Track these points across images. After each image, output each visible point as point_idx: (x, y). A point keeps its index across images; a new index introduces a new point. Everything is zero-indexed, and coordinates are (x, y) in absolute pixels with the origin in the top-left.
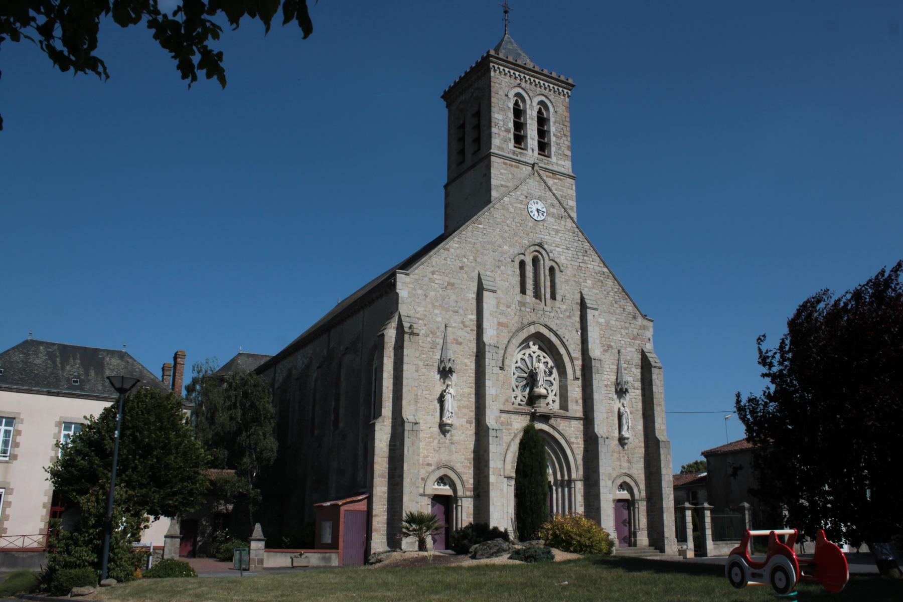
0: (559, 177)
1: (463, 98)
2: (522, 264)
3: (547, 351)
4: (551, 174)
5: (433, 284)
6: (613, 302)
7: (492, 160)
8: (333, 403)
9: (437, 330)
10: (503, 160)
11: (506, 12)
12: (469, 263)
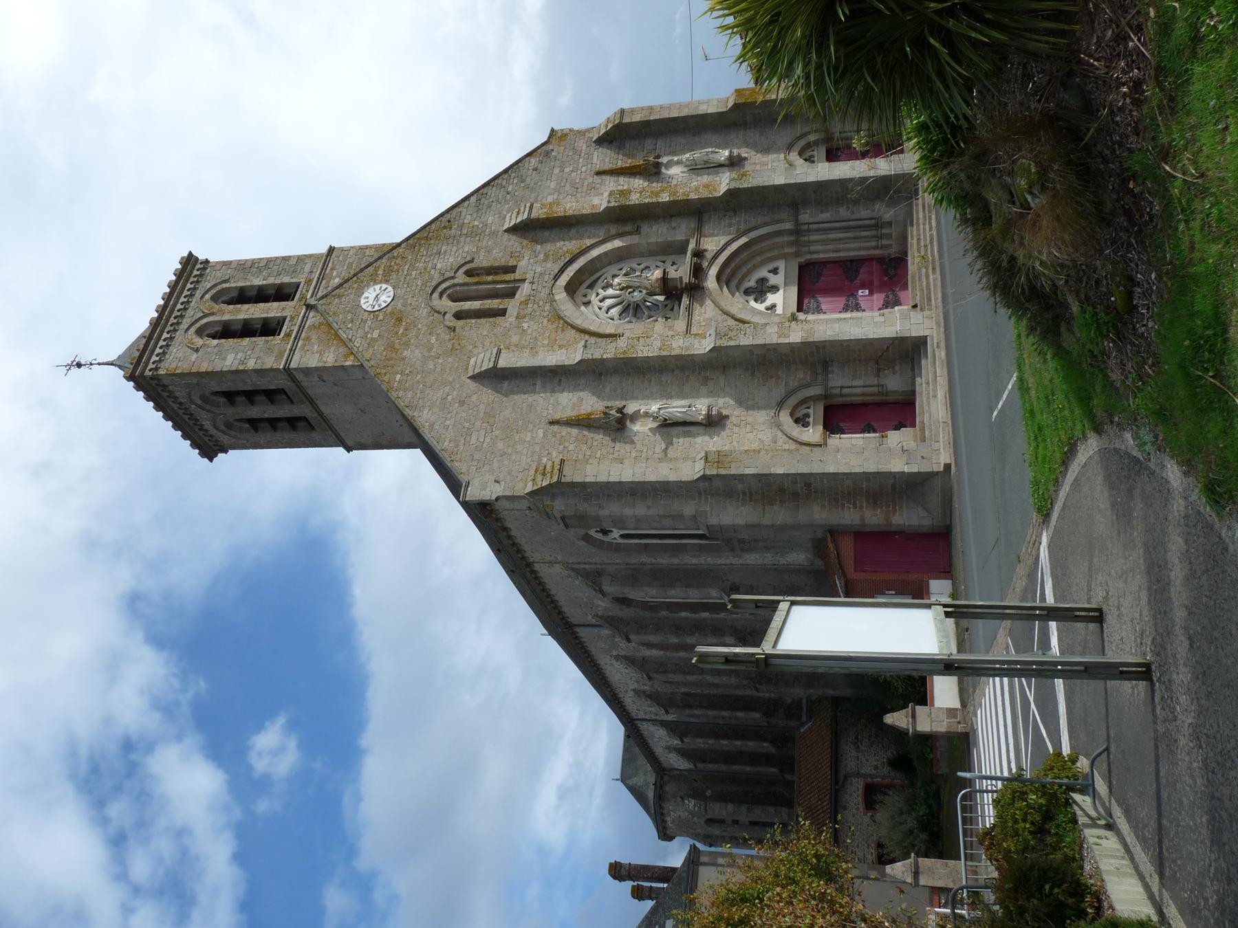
0: (329, 269)
1: (207, 425)
2: (459, 316)
3: (595, 277)
4: (324, 282)
5: (485, 445)
6: (522, 185)
7: (296, 366)
8: (683, 614)
9: (558, 436)
10: (296, 352)
11: (79, 365)
12: (455, 393)
